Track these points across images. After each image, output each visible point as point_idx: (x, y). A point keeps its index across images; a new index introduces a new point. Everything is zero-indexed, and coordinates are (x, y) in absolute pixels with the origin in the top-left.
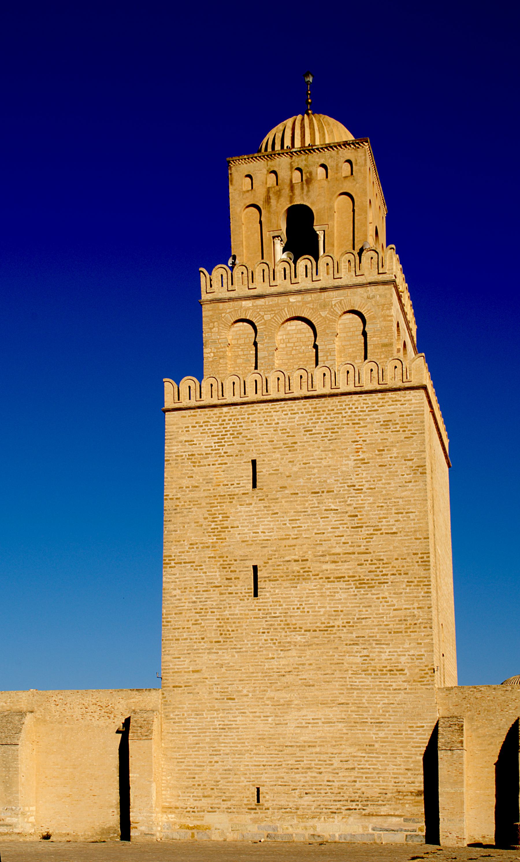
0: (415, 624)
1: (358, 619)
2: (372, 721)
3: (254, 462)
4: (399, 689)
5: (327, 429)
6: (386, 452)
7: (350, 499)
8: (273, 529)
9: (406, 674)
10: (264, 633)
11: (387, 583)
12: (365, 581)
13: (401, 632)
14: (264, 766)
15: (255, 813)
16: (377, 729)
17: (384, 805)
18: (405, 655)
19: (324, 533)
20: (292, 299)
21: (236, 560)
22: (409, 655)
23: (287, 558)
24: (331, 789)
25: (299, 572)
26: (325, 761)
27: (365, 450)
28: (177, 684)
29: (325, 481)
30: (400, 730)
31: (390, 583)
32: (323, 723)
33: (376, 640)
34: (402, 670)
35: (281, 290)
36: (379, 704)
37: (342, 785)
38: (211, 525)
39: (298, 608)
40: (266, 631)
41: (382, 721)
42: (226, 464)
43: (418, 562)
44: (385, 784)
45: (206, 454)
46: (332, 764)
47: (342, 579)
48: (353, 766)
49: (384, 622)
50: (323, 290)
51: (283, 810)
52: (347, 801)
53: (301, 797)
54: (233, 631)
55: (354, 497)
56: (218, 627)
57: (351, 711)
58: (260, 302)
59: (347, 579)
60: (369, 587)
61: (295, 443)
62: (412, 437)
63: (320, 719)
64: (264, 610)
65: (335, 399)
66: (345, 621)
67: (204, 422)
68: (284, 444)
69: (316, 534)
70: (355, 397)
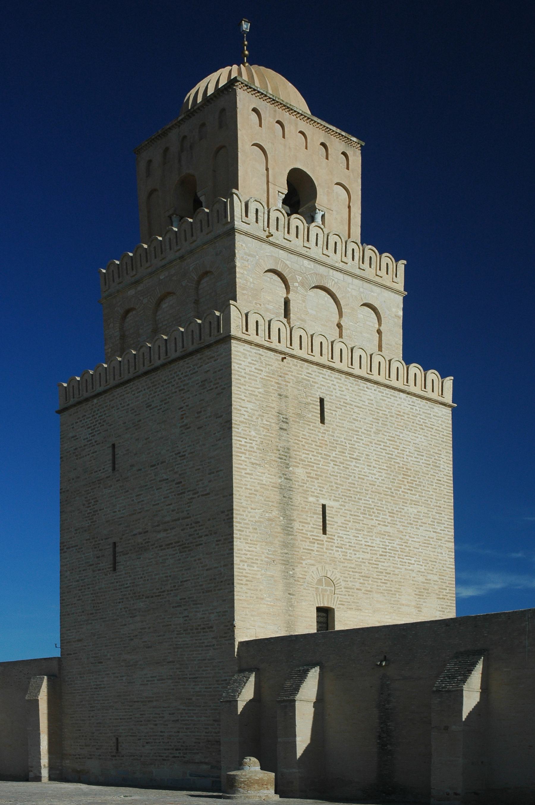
0: (222, 582)
1: (181, 582)
2: (191, 676)
3: (114, 445)
4: (210, 646)
7: (177, 466)
8: (125, 506)
9: (214, 631)
10: (120, 603)
11: (201, 544)
12: (187, 545)
13: (211, 591)
14: (121, 719)
15: (115, 760)
16: (194, 684)
17: (198, 753)
18: (213, 613)
19: (158, 504)
21: (102, 540)
22: (217, 612)
23: (135, 532)
24: (163, 739)
25: (142, 544)
26: (159, 714)
28: (69, 653)
29: (160, 453)
30: (209, 684)
31: (204, 544)
32: (158, 680)
33: (194, 601)
34: (212, 627)
36: (195, 660)
37: (170, 736)
38: (87, 511)
39: (141, 578)
40: (121, 601)
41: (197, 676)
43: (224, 520)
44: (199, 734)
46: (163, 717)
47: (171, 546)
48: (177, 719)
49: (199, 583)
51: (132, 758)
52: (173, 749)
53: (143, 746)
54: (101, 603)
55: (179, 464)
56: (93, 600)
57: (177, 669)
59: (174, 545)
60: (189, 551)
62: (222, 392)
63: (156, 677)
64: (120, 582)
66: (172, 585)
69: (154, 505)
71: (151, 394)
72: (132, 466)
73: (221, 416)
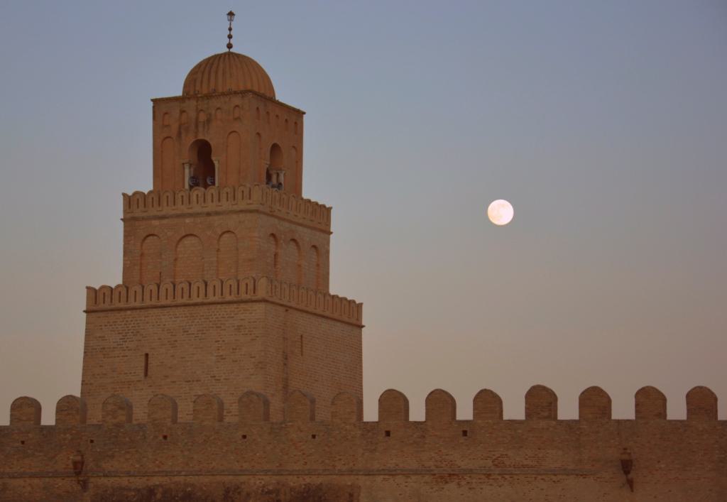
3: (147, 355)
5: (198, 331)
6: (237, 351)
20: (187, 221)
27: (223, 348)
35: (179, 212)
42: (127, 356)
45: (114, 348)
50: (208, 214)
58: (165, 221)
61: (176, 341)
65: (205, 308)
67: (114, 322)
68: (169, 342)
70: (219, 306)
71: (188, 323)
72: (167, 377)
73: (254, 357)
